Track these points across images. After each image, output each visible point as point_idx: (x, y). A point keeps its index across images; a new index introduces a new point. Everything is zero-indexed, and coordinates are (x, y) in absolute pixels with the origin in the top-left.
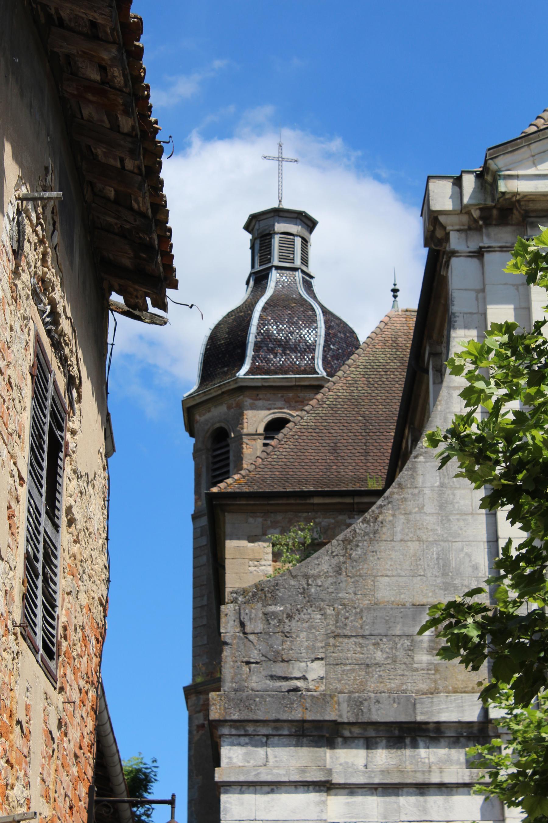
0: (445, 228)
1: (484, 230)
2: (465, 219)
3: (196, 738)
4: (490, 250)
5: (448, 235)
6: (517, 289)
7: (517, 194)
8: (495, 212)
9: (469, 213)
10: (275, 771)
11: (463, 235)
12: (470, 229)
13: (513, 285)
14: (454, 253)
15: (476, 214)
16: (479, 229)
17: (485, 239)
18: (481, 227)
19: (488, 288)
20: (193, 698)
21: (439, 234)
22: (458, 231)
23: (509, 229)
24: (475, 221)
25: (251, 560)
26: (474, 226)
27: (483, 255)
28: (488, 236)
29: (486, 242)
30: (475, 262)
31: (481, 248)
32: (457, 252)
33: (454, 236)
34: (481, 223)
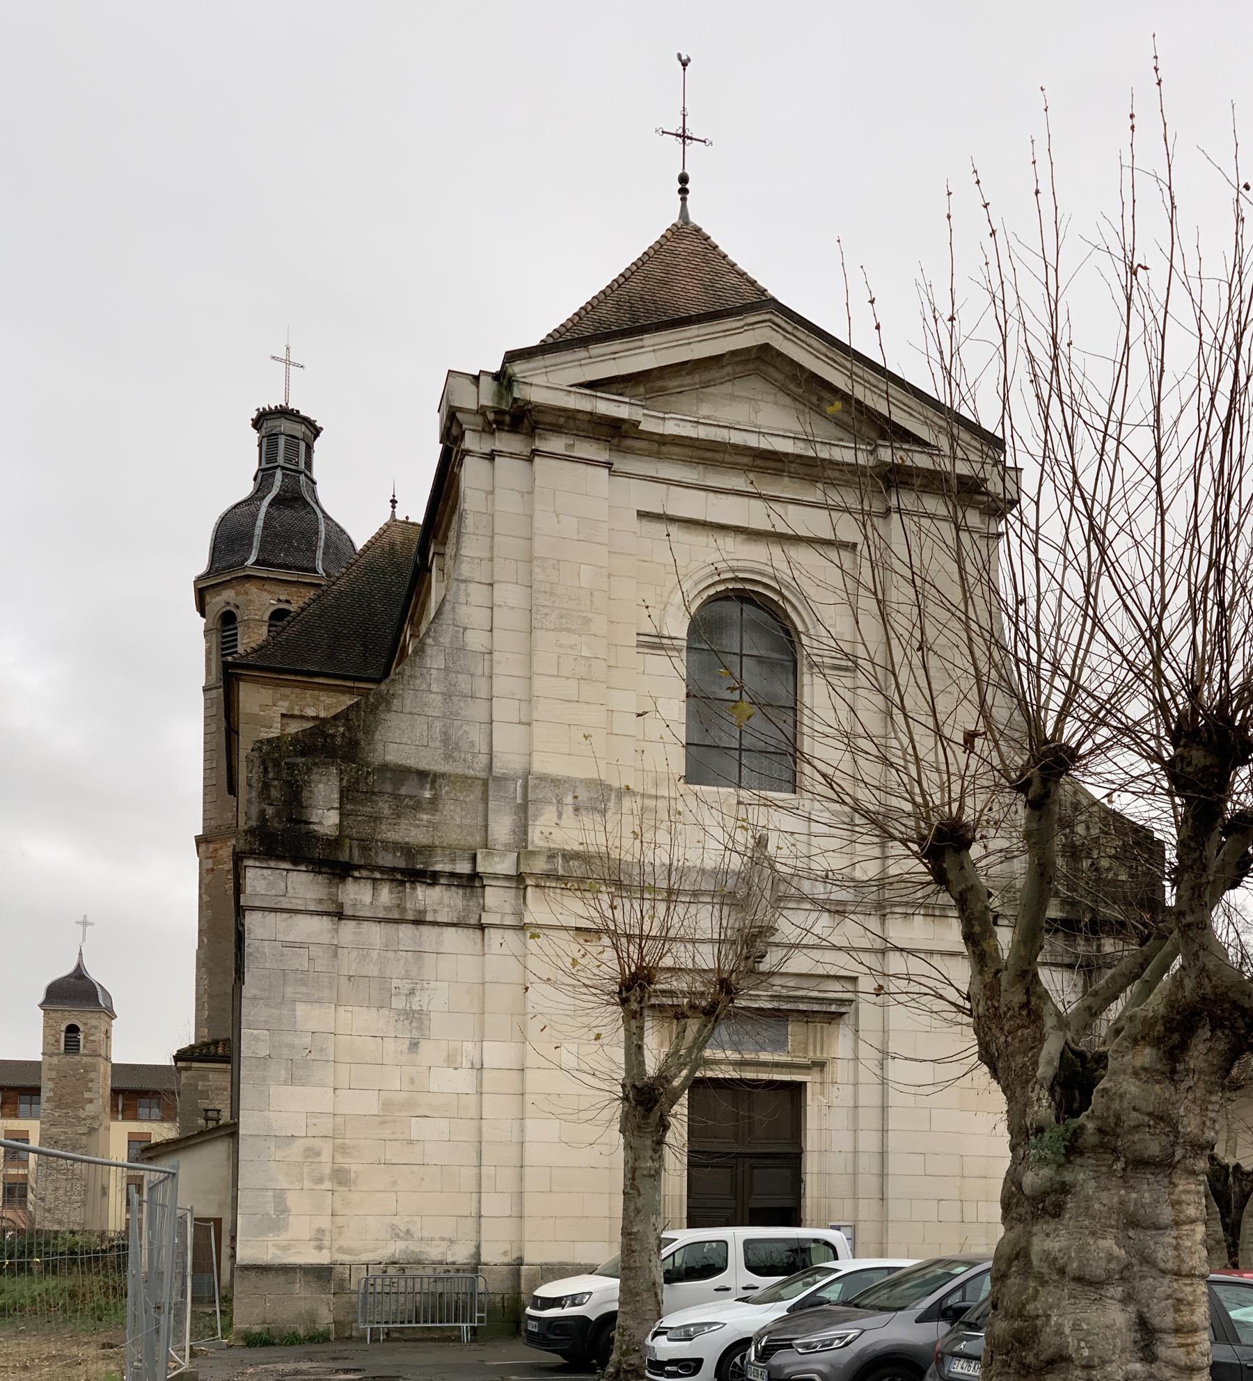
0: (461, 426)
1: (497, 434)
2: (479, 419)
3: (206, 881)
4: (501, 454)
5: (463, 433)
6: (523, 496)
7: (529, 402)
8: (507, 418)
9: (484, 414)
10: (294, 901)
11: (477, 435)
12: (484, 431)
13: (519, 492)
14: (467, 452)
15: (491, 416)
16: (492, 433)
17: (497, 443)
18: (494, 430)
19: (497, 491)
20: (203, 847)
21: (455, 431)
22: (473, 431)
23: (518, 437)
24: (490, 424)
25: (262, 726)
26: (487, 429)
27: (494, 459)
28: (500, 441)
29: (498, 446)
30: (485, 464)
31: (493, 451)
32: (471, 451)
33: (468, 434)
34: (494, 426)
